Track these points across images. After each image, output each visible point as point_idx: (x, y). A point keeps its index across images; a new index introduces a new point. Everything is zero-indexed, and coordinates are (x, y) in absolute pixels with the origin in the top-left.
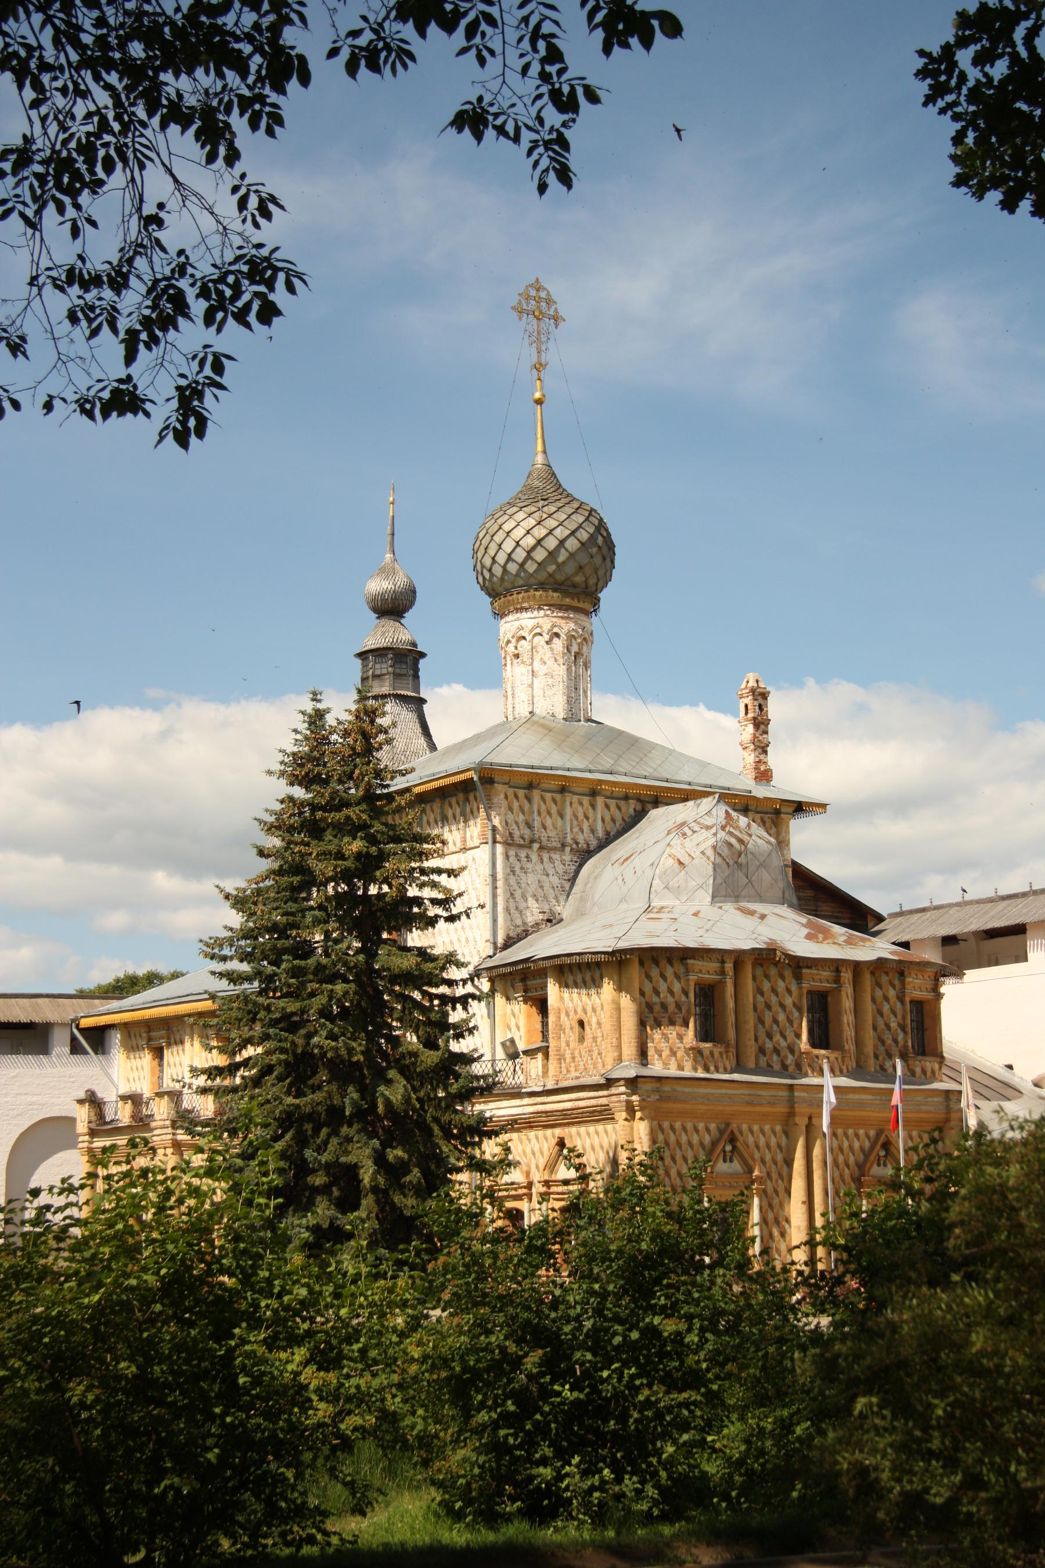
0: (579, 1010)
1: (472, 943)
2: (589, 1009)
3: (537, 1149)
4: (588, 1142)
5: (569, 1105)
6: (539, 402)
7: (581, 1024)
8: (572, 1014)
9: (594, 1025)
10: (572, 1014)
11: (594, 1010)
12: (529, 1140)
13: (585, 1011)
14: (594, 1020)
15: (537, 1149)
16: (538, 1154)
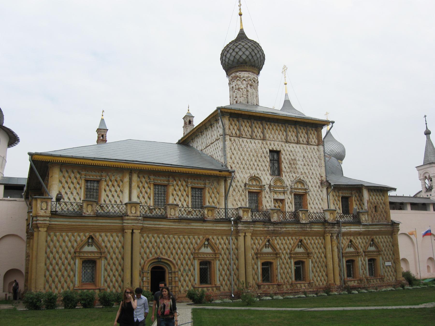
0: (376, 203)
1: (315, 175)
2: (379, 203)
3: (361, 241)
4: (379, 240)
5: (378, 229)
6: (241, 15)
7: (376, 207)
8: (373, 203)
9: (381, 208)
10: (373, 203)
11: (381, 203)
12: (358, 239)
13: (378, 203)
14: (381, 206)
15: (361, 241)
16: (361, 243)
